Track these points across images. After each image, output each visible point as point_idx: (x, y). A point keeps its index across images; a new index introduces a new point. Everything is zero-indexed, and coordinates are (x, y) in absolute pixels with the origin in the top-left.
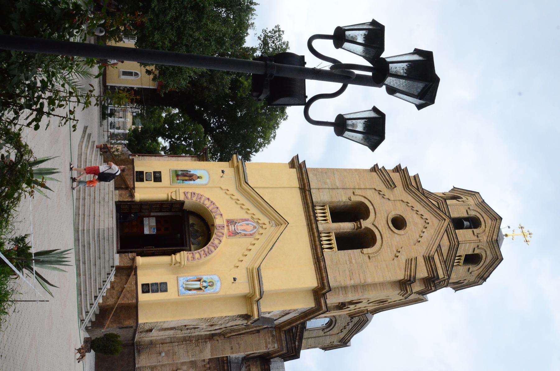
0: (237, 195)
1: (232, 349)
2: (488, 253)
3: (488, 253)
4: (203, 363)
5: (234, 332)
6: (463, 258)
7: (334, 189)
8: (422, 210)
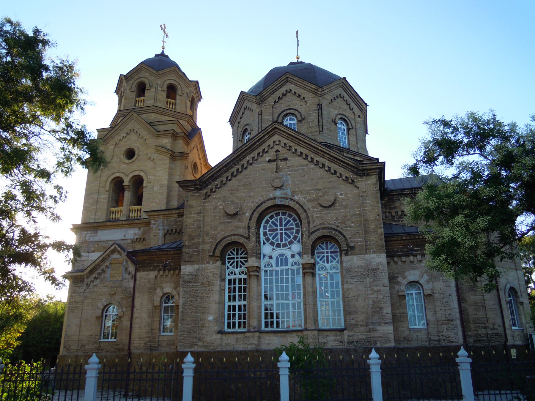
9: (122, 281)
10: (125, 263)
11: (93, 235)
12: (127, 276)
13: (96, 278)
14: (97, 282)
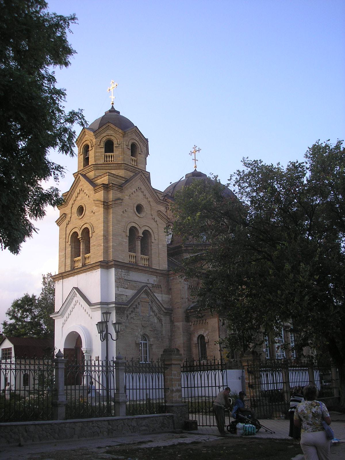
0: (65, 318)
1: (178, 308)
2: (104, 134)
3: (104, 134)
4: (192, 326)
5: (161, 308)
6: (108, 154)
7: (65, 255)
8: (75, 194)
9: (149, 317)
10: (150, 303)
11: (126, 274)
12: (152, 313)
13: (132, 311)
14: (133, 315)
